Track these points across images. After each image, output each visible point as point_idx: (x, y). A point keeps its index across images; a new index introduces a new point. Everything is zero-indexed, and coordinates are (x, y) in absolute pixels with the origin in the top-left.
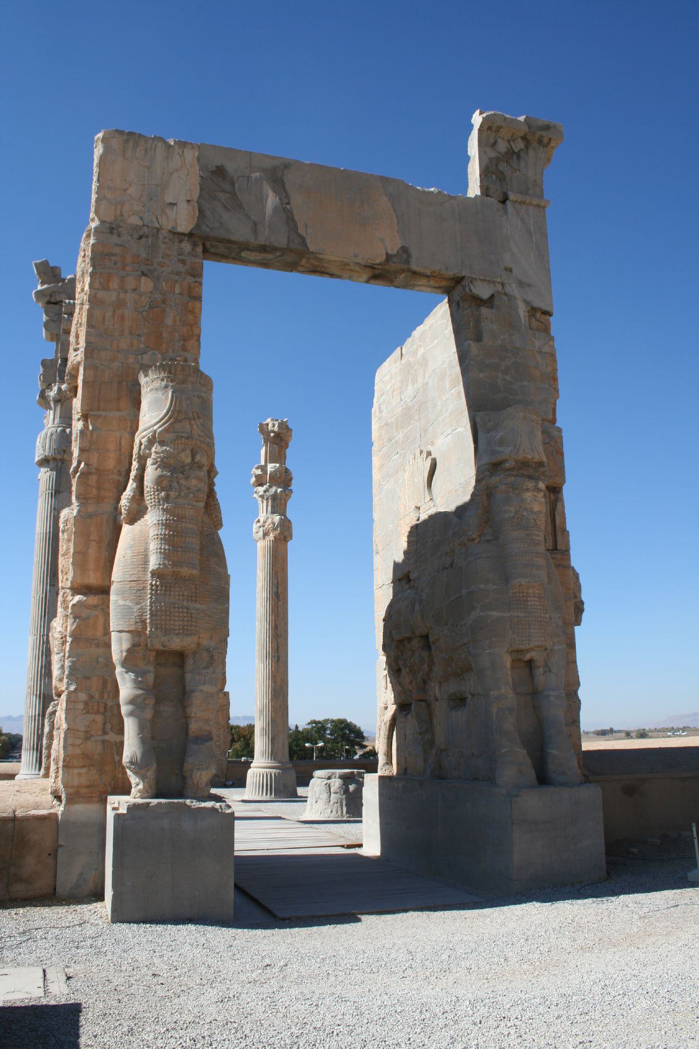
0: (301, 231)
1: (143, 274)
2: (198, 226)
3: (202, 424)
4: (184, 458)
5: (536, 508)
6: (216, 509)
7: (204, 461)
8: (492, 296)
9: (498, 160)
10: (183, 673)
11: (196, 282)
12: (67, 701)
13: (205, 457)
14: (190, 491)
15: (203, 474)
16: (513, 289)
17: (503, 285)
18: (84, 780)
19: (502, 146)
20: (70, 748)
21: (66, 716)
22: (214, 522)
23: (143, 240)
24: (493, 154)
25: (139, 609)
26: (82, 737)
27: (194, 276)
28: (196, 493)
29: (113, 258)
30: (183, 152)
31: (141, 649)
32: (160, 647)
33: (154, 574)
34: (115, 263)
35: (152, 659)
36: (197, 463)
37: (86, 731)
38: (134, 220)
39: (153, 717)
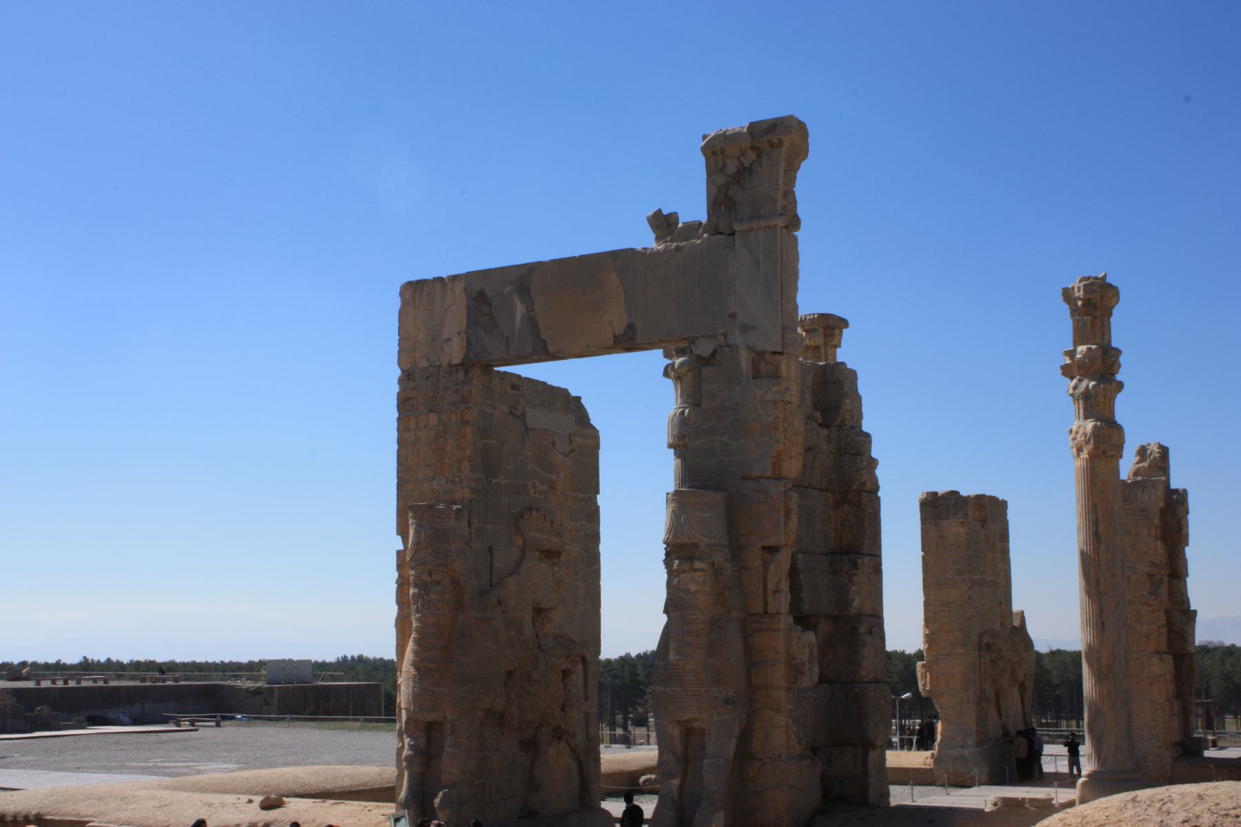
0: (543, 336)
1: (432, 411)
2: (466, 355)
5: (692, 588)
8: (715, 350)
9: (728, 185)
11: (466, 408)
16: (737, 338)
17: (725, 335)
19: (732, 167)
23: (430, 379)
24: (721, 180)
27: (464, 403)
29: (411, 402)
30: (454, 287)
32: (421, 720)
34: (412, 406)
38: (423, 364)
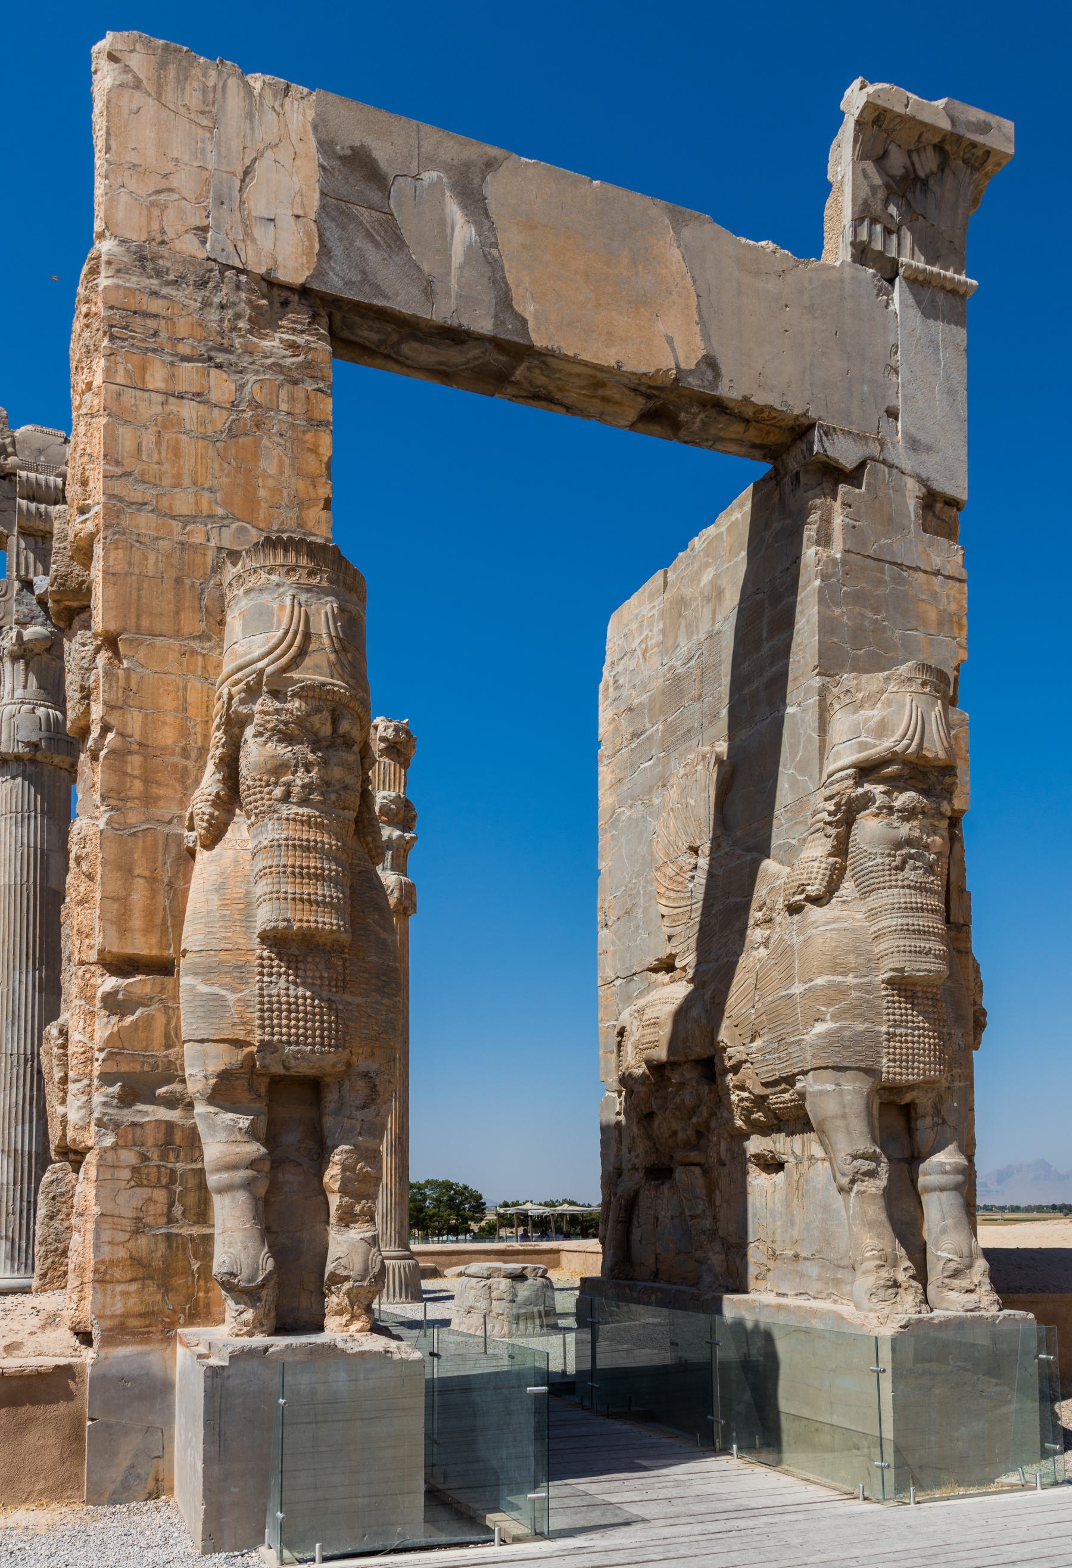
3: (351, 664)
4: (317, 724)
6: (373, 826)
7: (356, 734)
10: (321, 1117)
12: (99, 1166)
13: (358, 727)
14: (330, 789)
15: (352, 758)
18: (134, 1304)
20: (106, 1249)
21: (97, 1191)
22: (370, 851)
25: (239, 1000)
26: (129, 1229)
28: (342, 792)
31: (244, 1073)
33: (265, 938)
35: (263, 1090)
36: (343, 736)
37: (136, 1218)
39: (267, 1192)
